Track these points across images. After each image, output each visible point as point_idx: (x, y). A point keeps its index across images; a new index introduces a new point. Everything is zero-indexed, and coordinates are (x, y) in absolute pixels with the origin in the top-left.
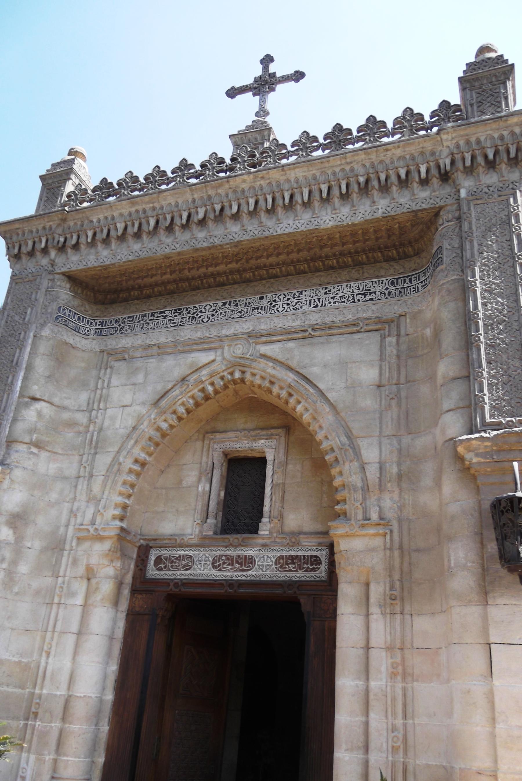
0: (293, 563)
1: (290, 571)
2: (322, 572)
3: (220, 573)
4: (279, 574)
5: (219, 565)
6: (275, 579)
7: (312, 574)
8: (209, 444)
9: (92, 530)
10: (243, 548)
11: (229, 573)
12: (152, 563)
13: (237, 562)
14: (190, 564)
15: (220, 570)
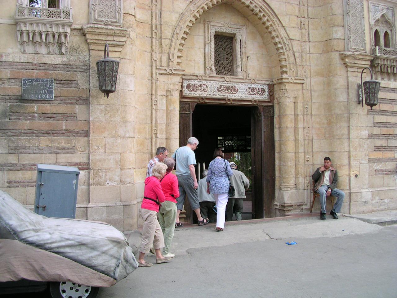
0: (254, 91)
1: (253, 94)
2: (265, 97)
3: (222, 94)
4: (249, 96)
5: (221, 90)
7: (262, 96)
8: (208, 27)
9: (168, 71)
12: (186, 87)
13: (229, 89)
14: (206, 89)
15: (222, 93)
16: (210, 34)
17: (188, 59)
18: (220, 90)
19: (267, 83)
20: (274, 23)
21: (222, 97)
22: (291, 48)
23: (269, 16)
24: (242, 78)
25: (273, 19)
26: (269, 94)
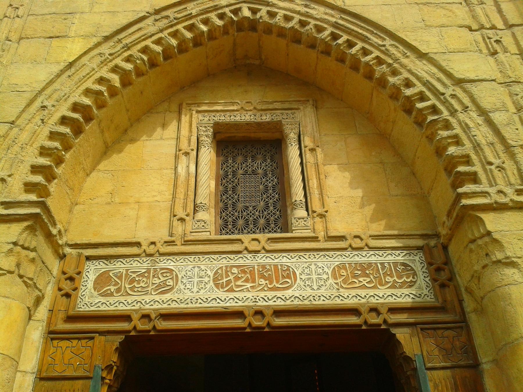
0: (367, 276)
1: (364, 287)
3: (231, 295)
4: (345, 293)
5: (228, 282)
6: (338, 301)
10: (268, 255)
11: (249, 295)
13: (262, 276)
15: (231, 290)
16: (194, 130)
17: (117, 200)
18: (225, 280)
19: (420, 242)
20: (386, 53)
21: (231, 305)
22: (466, 101)
23: (365, 39)
24: (313, 235)
25: (380, 43)
26: (434, 280)
